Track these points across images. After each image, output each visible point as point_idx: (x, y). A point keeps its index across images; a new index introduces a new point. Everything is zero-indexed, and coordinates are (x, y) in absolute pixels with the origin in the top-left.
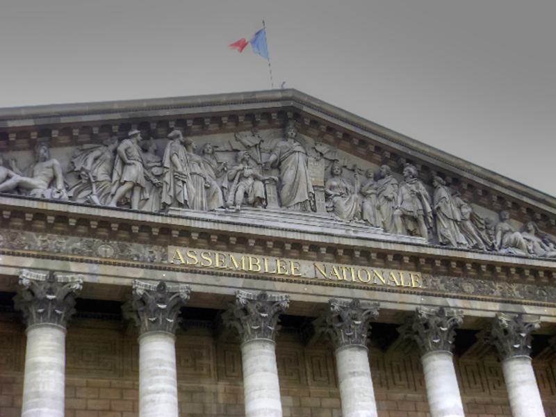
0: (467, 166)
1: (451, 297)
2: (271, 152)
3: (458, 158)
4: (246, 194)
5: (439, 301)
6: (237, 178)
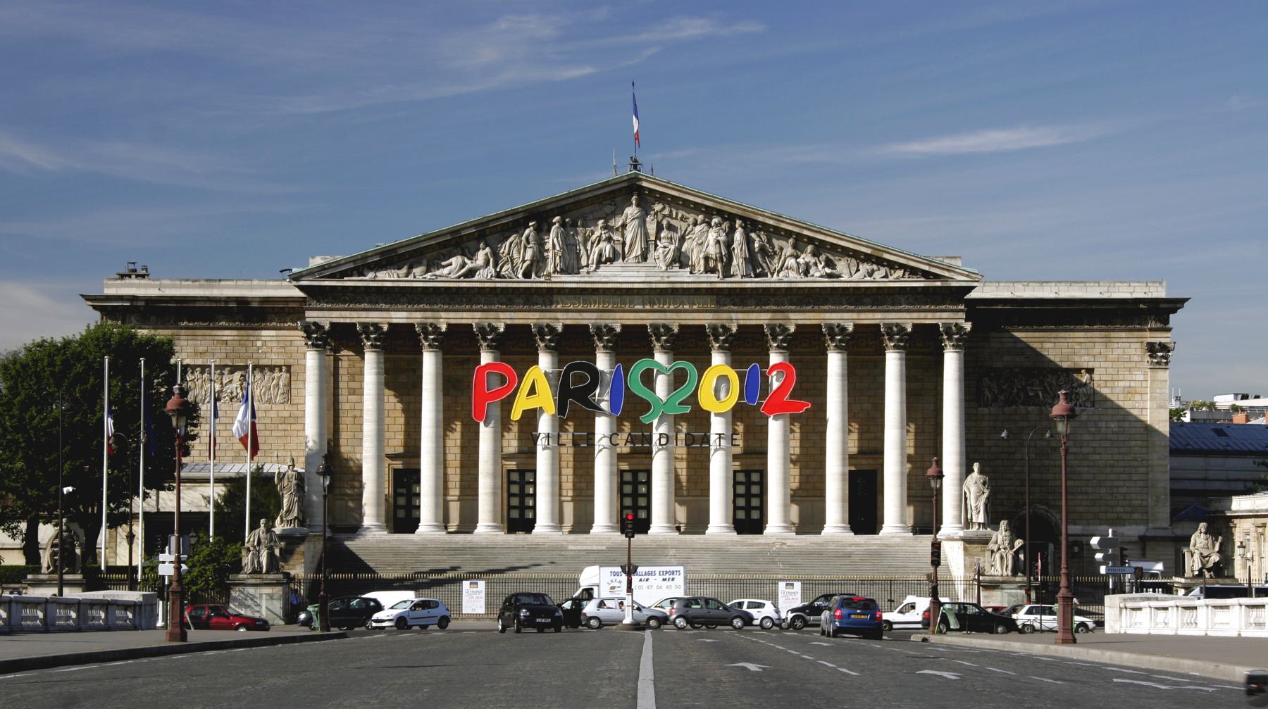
4: (600, 255)
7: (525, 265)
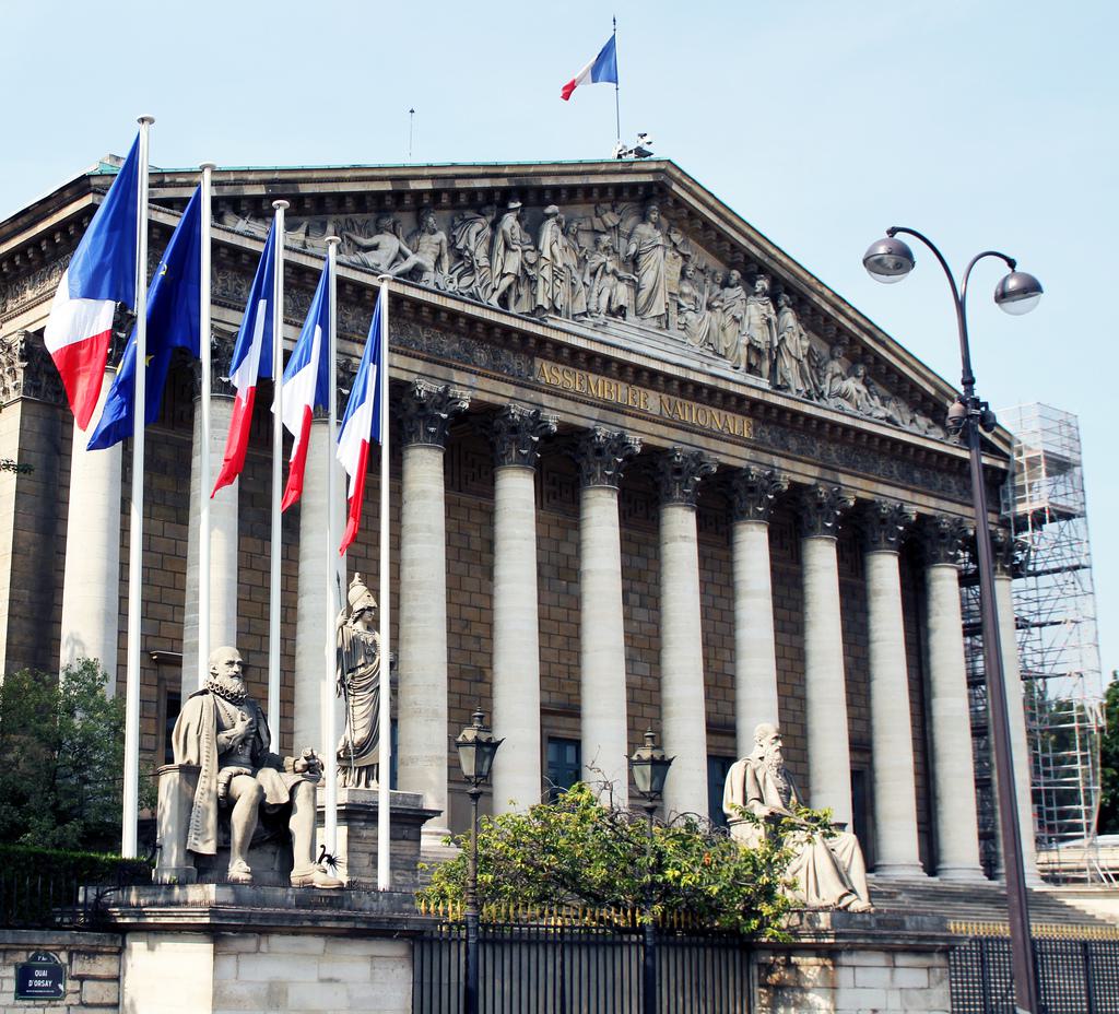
0: (819, 288)
1: (777, 455)
2: (629, 237)
3: (812, 276)
5: (765, 458)
6: (599, 273)
7: (507, 281)
